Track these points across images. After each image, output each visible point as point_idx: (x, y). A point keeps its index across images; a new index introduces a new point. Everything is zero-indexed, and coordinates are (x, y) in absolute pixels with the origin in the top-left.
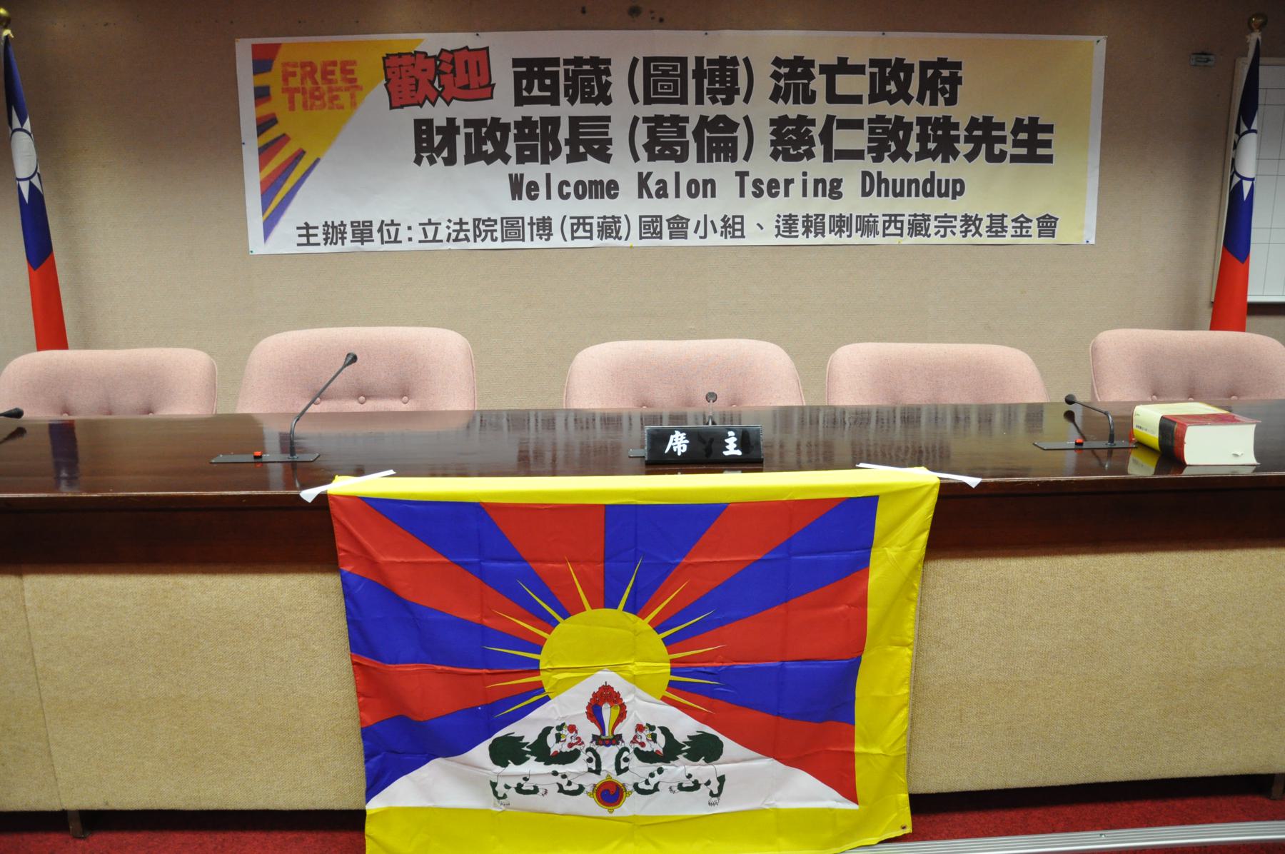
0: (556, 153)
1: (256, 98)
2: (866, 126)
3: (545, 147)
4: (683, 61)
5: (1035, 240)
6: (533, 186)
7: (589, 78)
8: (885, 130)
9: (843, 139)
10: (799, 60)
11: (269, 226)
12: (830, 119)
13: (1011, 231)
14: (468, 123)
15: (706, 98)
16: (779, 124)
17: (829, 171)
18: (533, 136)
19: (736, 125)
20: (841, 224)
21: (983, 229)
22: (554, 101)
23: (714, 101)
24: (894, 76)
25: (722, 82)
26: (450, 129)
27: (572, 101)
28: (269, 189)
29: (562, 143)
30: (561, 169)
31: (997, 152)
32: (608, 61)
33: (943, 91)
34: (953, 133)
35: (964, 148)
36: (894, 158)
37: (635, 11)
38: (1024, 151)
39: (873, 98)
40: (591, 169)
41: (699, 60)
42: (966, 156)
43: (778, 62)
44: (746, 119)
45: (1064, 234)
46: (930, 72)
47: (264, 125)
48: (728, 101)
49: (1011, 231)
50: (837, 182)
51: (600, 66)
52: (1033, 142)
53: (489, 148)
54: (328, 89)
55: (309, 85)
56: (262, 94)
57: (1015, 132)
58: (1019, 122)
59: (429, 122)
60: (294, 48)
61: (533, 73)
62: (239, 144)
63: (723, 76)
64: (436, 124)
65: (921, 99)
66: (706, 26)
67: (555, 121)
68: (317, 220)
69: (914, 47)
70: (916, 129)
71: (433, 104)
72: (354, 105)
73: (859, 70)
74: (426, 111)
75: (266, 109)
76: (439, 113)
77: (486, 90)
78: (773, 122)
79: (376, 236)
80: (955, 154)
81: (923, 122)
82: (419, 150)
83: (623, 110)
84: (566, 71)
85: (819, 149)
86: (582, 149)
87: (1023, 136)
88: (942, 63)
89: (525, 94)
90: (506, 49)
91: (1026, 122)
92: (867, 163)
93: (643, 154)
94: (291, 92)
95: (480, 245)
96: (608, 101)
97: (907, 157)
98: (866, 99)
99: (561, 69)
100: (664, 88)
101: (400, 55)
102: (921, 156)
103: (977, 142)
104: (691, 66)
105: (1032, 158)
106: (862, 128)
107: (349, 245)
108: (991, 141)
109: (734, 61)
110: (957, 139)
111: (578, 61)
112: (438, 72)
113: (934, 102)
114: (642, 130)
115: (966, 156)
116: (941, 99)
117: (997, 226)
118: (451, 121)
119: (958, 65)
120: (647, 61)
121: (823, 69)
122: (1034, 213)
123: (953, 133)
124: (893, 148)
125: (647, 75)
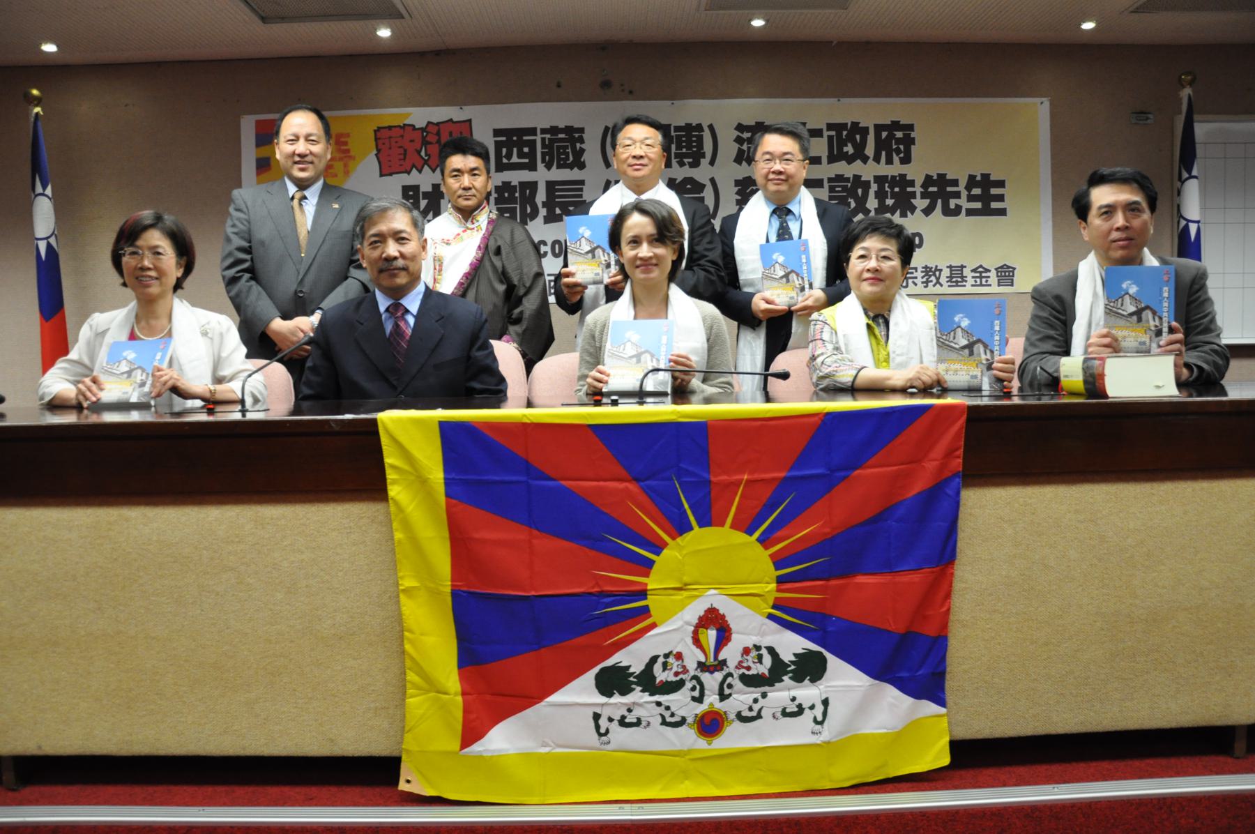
0: (534, 215)
1: (258, 168)
2: (826, 185)
3: (523, 210)
5: (995, 289)
8: (845, 189)
13: (970, 281)
15: (674, 161)
18: (514, 200)
19: (701, 187)
21: (943, 280)
22: (532, 167)
23: (681, 164)
24: (851, 138)
25: (689, 147)
27: (549, 167)
29: (540, 205)
31: (952, 206)
32: (582, 130)
33: (898, 151)
34: (909, 189)
35: (921, 203)
37: (606, 85)
38: (978, 205)
39: (832, 159)
42: (923, 211)
43: (740, 128)
44: (713, 181)
46: (884, 134)
48: (695, 164)
49: (970, 281)
51: (574, 135)
52: (987, 197)
57: (968, 188)
59: (416, 188)
61: (513, 141)
63: (689, 142)
64: (422, 189)
65: (877, 159)
66: (673, 96)
67: (533, 186)
69: (869, 112)
71: (420, 171)
72: (347, 173)
74: (413, 178)
78: (737, 183)
80: (913, 209)
81: (880, 180)
84: (543, 139)
86: (558, 211)
87: (977, 191)
88: (896, 125)
89: (505, 161)
91: (979, 178)
96: (582, 166)
98: (824, 160)
99: (538, 138)
101: (390, 128)
103: (933, 198)
105: (986, 211)
106: (822, 186)
108: (946, 197)
109: (699, 127)
110: (913, 195)
111: (554, 130)
112: (425, 143)
113: (889, 161)
115: (923, 211)
116: (896, 159)
117: (957, 275)
119: (911, 127)
122: (992, 263)
123: (909, 189)
124: (853, 205)
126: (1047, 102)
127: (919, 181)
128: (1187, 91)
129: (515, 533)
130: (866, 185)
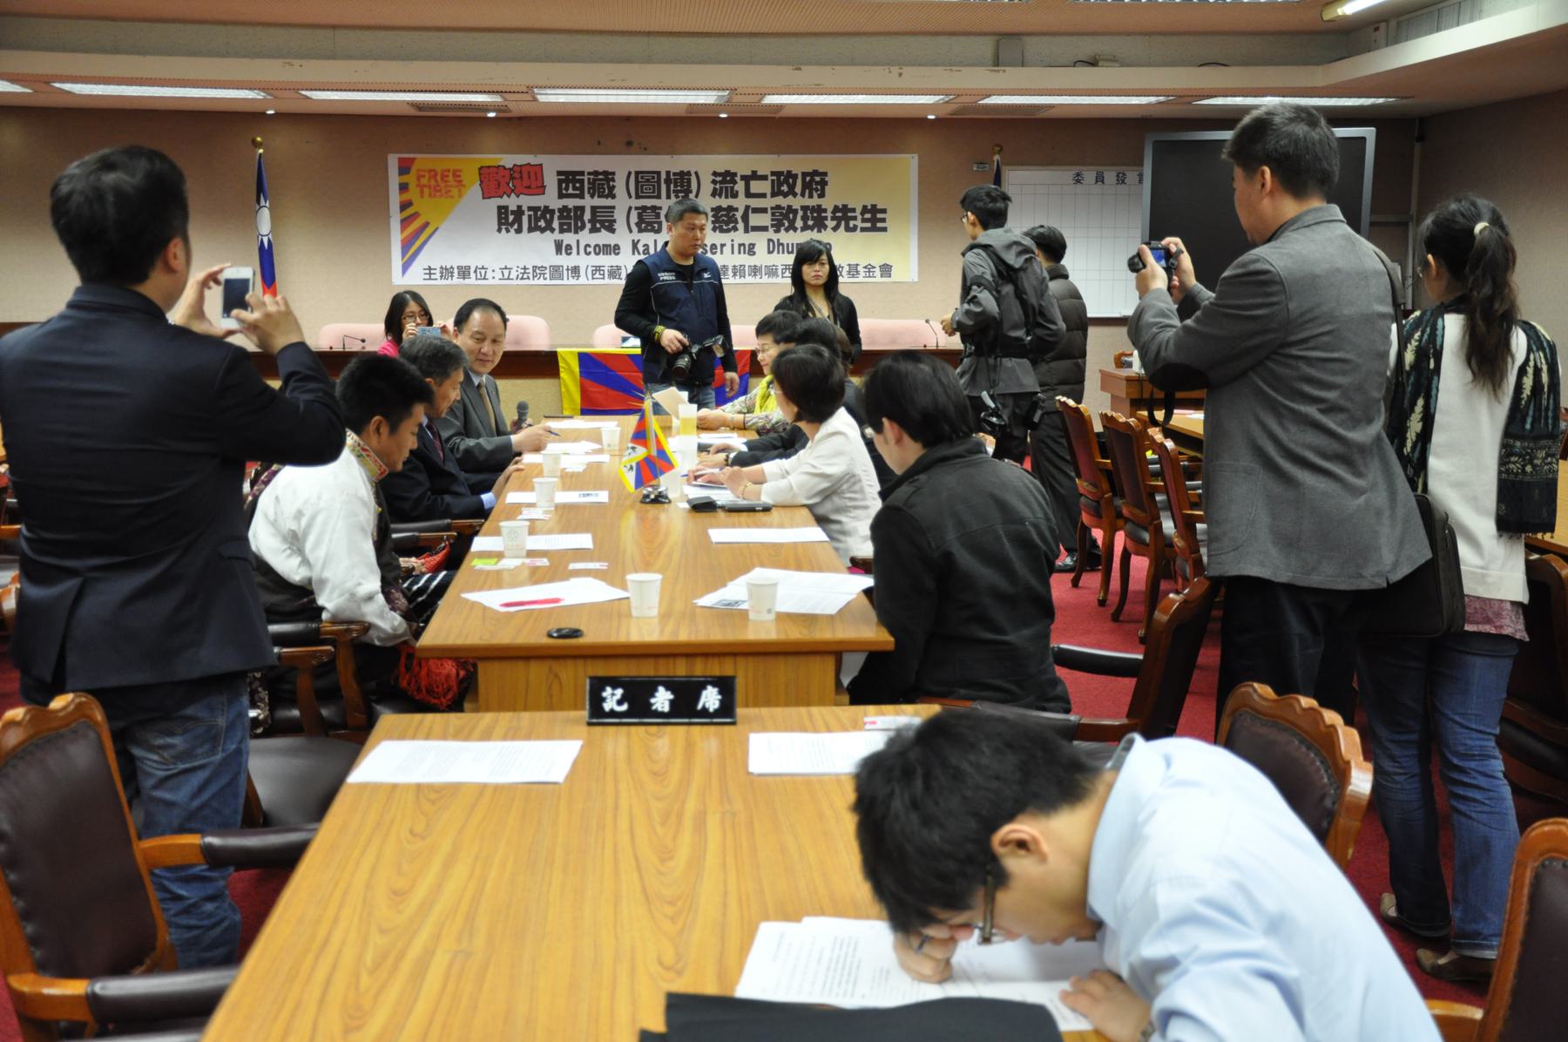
4: (659, 173)
6: (569, 247)
7: (602, 183)
9: (755, 220)
10: (727, 173)
11: (406, 267)
12: (747, 207)
14: (530, 209)
16: (716, 210)
17: (748, 238)
20: (755, 270)
22: (581, 196)
26: (519, 213)
28: (406, 245)
30: (586, 237)
35: (831, 224)
36: (787, 230)
37: (629, 144)
39: (774, 195)
40: (603, 237)
41: (668, 173)
43: (715, 174)
45: (896, 275)
47: (404, 206)
50: (752, 246)
51: (609, 176)
52: (874, 219)
53: (542, 224)
54: (444, 186)
55: (433, 182)
56: (404, 188)
58: (865, 207)
59: (506, 208)
60: (423, 160)
61: (568, 179)
62: (388, 217)
65: (803, 195)
66: (672, 152)
67: (582, 209)
68: (436, 265)
69: (798, 164)
70: (800, 213)
72: (460, 196)
73: (764, 178)
74: (504, 201)
75: (406, 196)
76: (512, 202)
77: (541, 189)
79: (473, 275)
80: (825, 227)
81: (804, 208)
82: (500, 224)
83: (623, 203)
85: (741, 225)
87: (868, 216)
88: (816, 173)
90: (552, 165)
92: (771, 234)
93: (635, 229)
94: (421, 187)
95: (536, 282)
96: (613, 197)
97: (795, 230)
100: (647, 189)
102: (803, 229)
103: (839, 220)
104: (663, 176)
105: (874, 229)
107: (456, 280)
109: (689, 173)
111: (596, 173)
113: (811, 196)
114: (634, 215)
118: (519, 207)
119: (825, 174)
120: (637, 173)
121: (743, 178)
122: (877, 262)
125: (637, 182)
126: (916, 156)
127: (830, 209)
128: (997, 157)
129: (602, 389)
130: (795, 212)
